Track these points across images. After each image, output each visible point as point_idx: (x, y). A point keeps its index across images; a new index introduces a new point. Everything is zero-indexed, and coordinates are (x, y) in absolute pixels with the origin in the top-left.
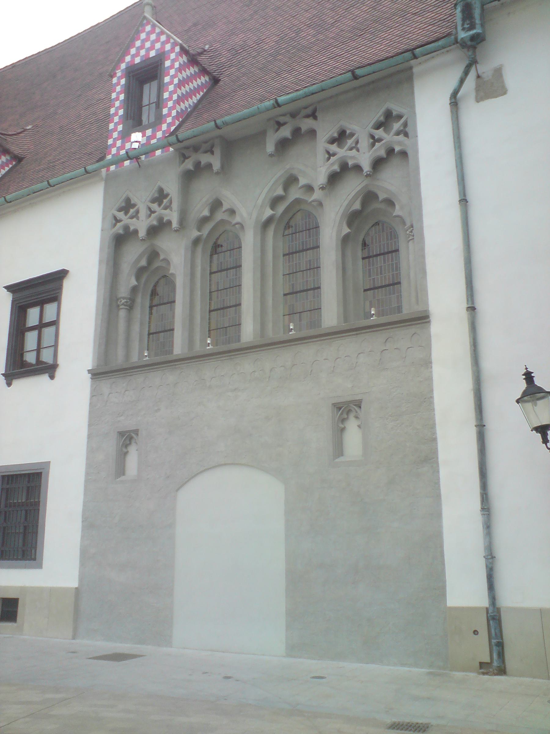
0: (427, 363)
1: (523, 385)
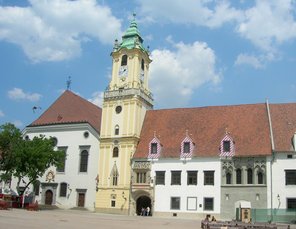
0: (267, 191)
1: (278, 196)
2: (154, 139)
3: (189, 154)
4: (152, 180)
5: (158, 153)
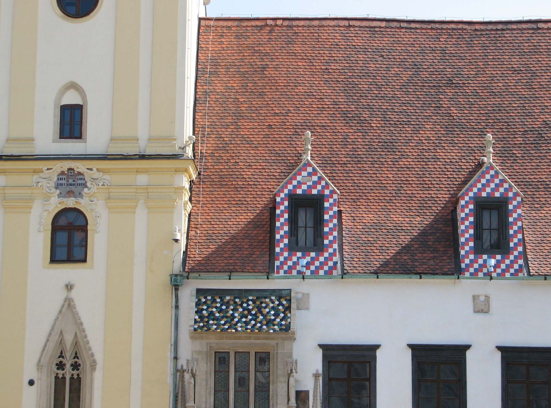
2: (304, 174)
3: (507, 262)
4: (298, 393)
5: (331, 250)
